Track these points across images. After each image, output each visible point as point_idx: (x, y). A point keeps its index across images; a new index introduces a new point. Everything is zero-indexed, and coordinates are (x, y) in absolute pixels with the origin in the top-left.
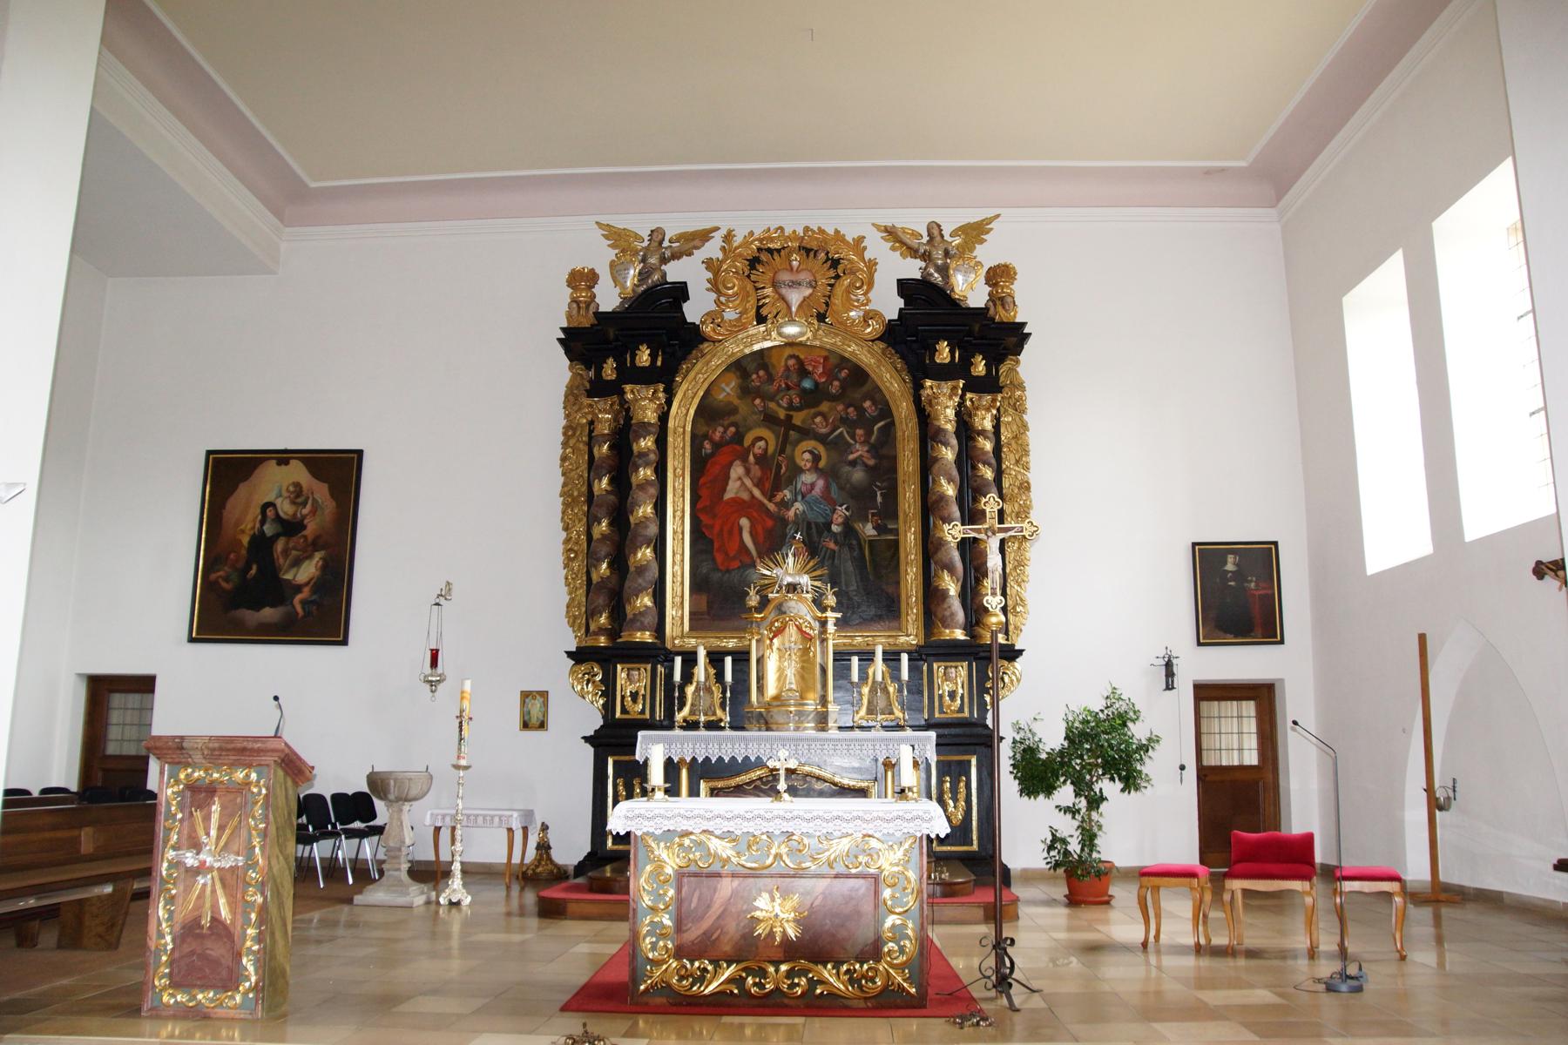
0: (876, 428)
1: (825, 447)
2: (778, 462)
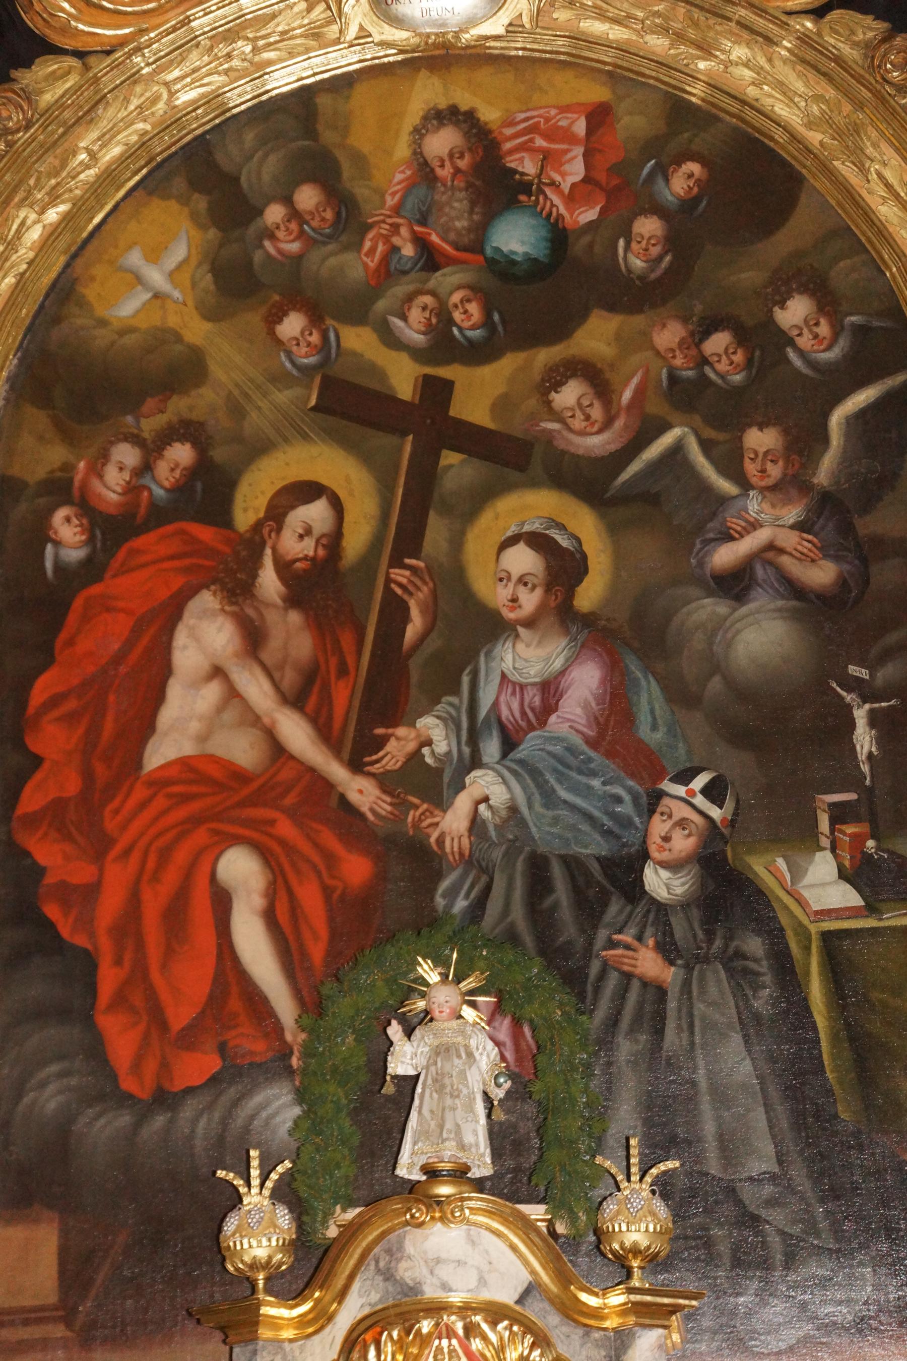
0: (837, 418)
1: (602, 516)
2: (387, 589)
